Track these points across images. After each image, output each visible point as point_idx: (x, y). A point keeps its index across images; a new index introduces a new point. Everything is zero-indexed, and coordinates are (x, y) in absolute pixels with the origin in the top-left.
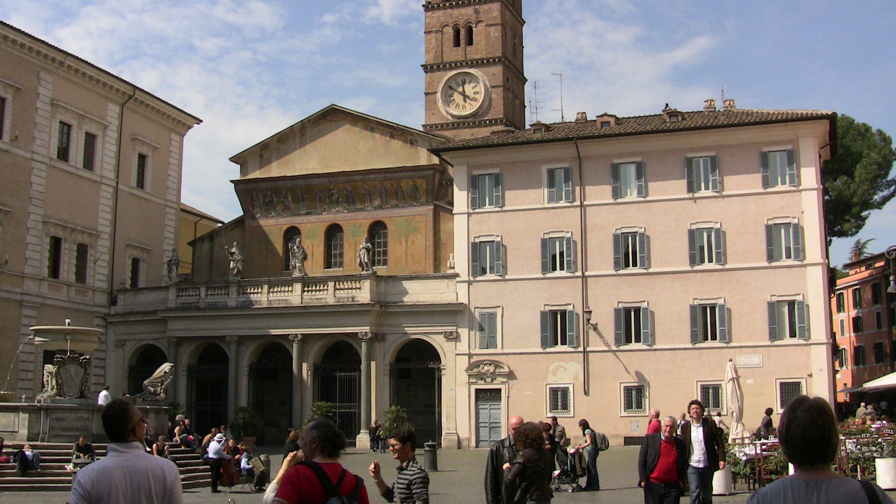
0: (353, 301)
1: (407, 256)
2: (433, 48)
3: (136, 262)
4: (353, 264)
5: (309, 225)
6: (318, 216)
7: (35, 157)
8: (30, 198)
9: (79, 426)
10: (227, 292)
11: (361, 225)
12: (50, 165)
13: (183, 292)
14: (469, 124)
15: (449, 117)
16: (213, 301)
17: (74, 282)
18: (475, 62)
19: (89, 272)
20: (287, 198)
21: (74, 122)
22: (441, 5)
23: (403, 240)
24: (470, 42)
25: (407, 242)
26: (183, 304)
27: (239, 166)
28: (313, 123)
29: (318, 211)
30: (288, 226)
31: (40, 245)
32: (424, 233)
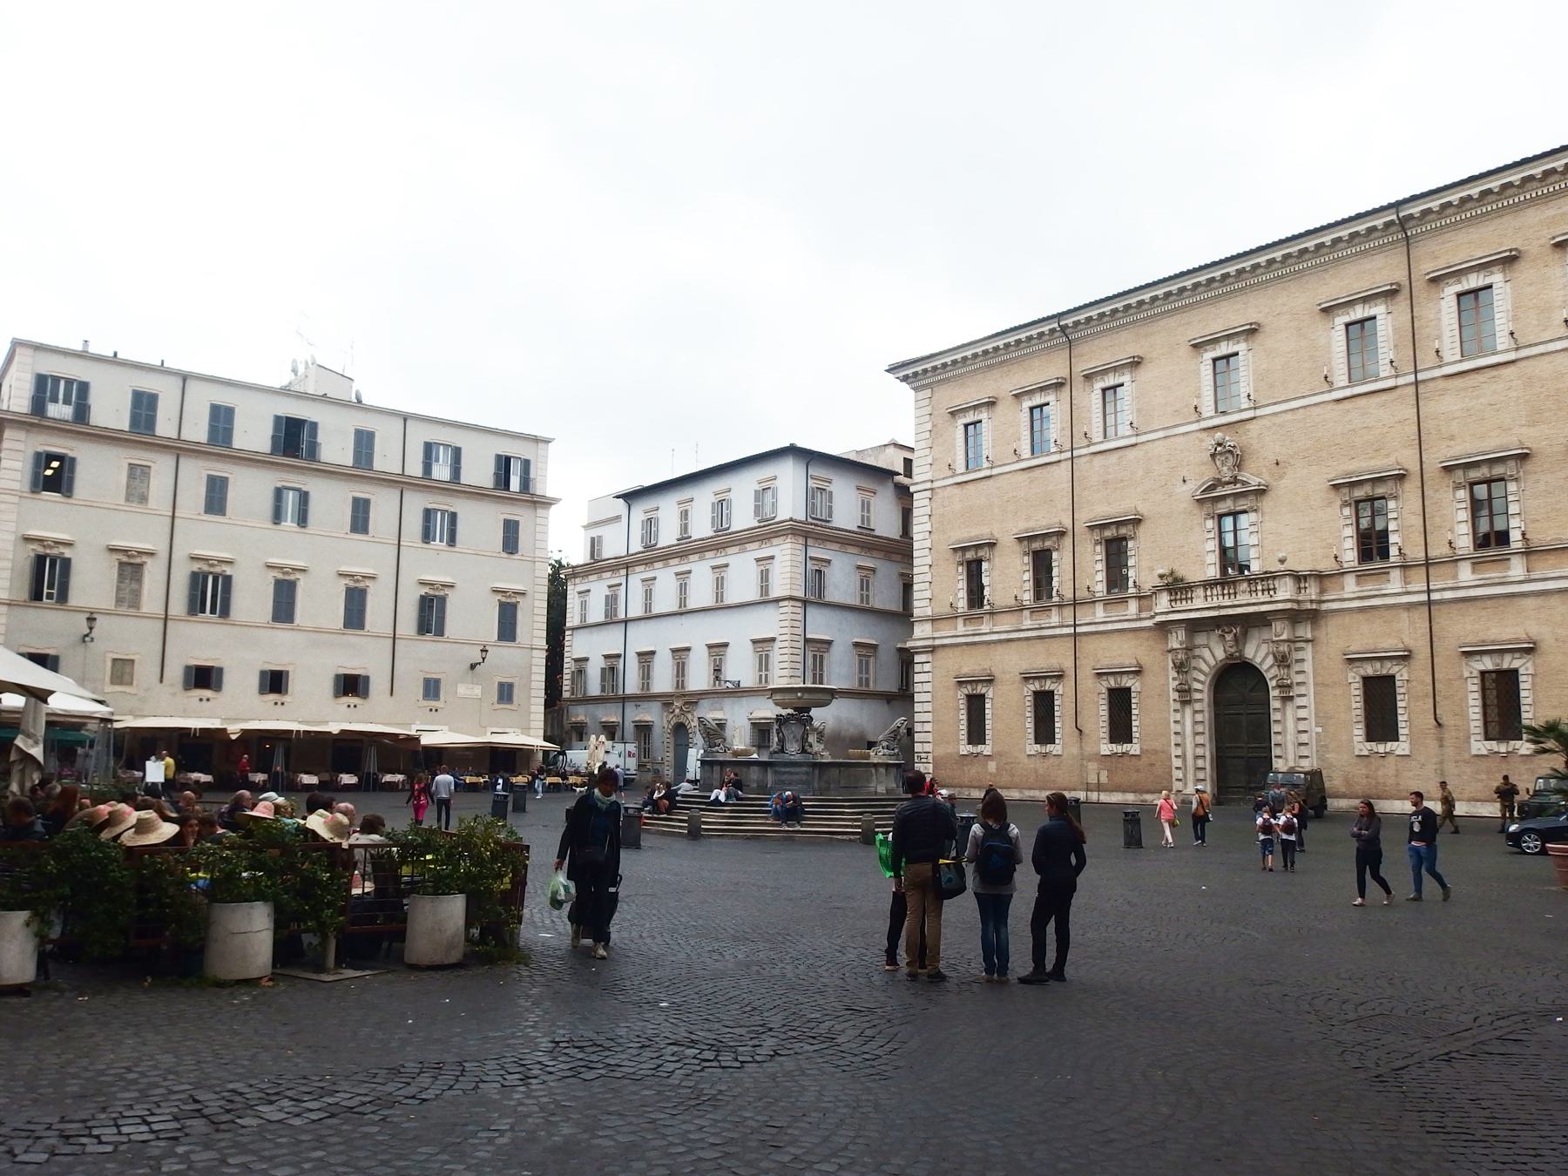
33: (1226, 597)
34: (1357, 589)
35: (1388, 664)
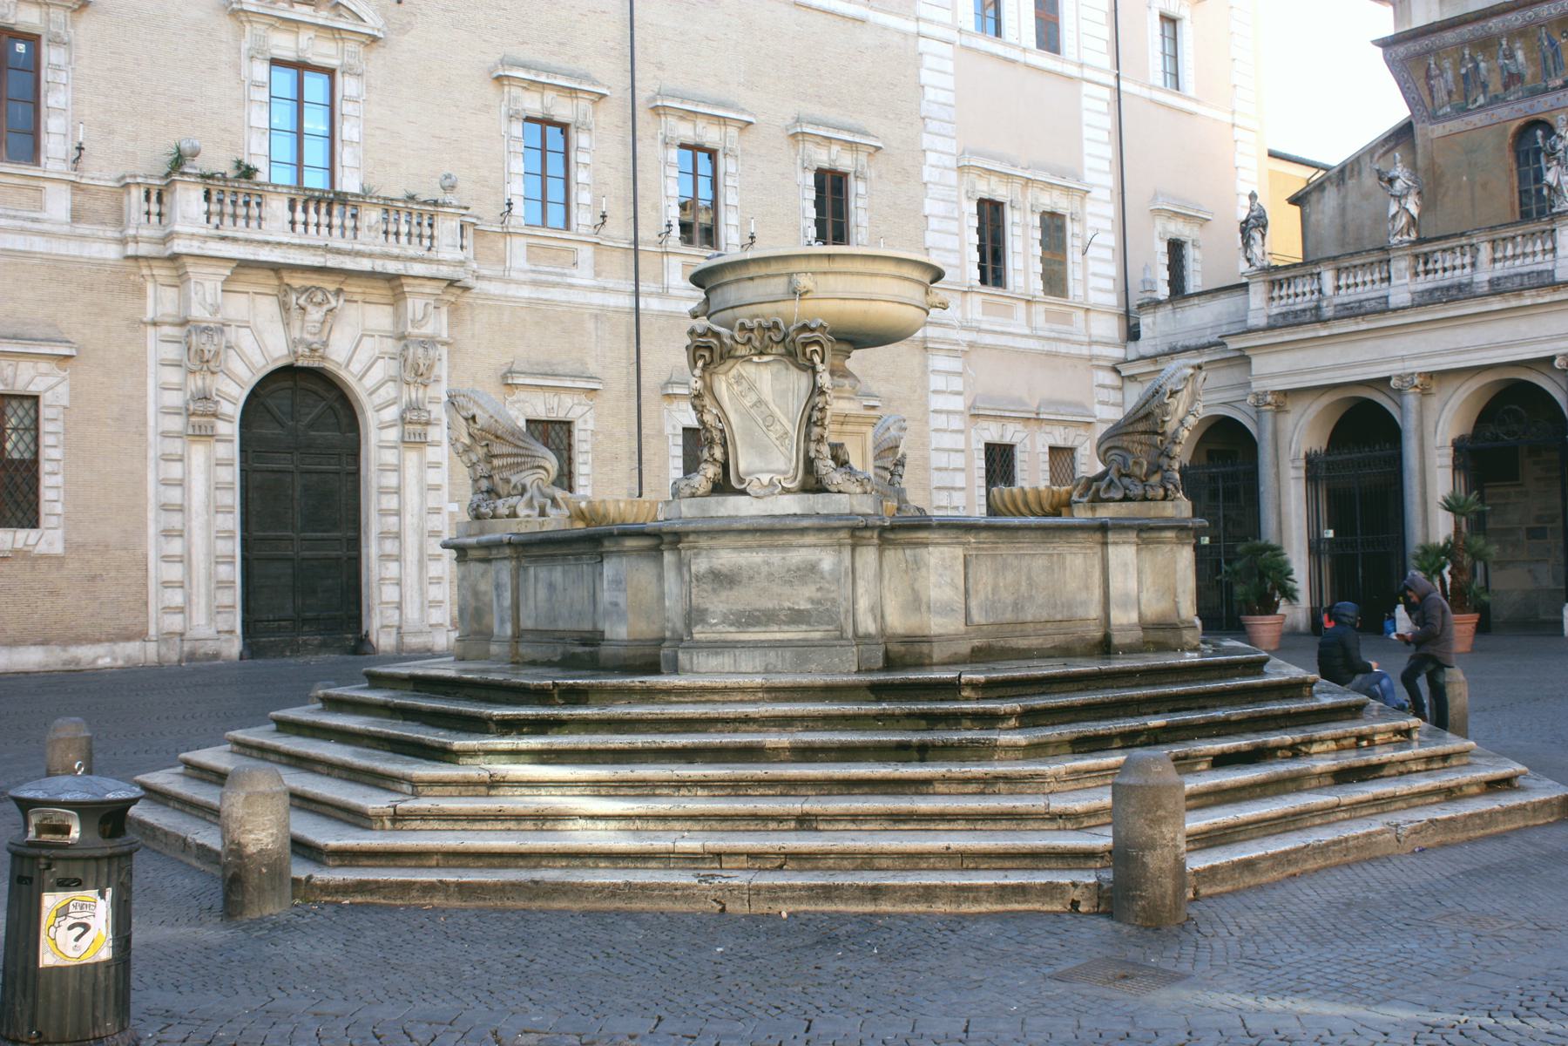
3: (1176, 248)
7: (924, 28)
8: (923, 119)
9: (804, 605)
10: (1385, 275)
12: (962, 46)
13: (1281, 286)
16: (1353, 298)
17: (1042, 294)
19: (1074, 273)
20: (1512, 56)
27: (1391, 8)
30: (1516, 124)
31: (957, 219)
33: (241, 222)
34: (527, 266)
35: (568, 400)
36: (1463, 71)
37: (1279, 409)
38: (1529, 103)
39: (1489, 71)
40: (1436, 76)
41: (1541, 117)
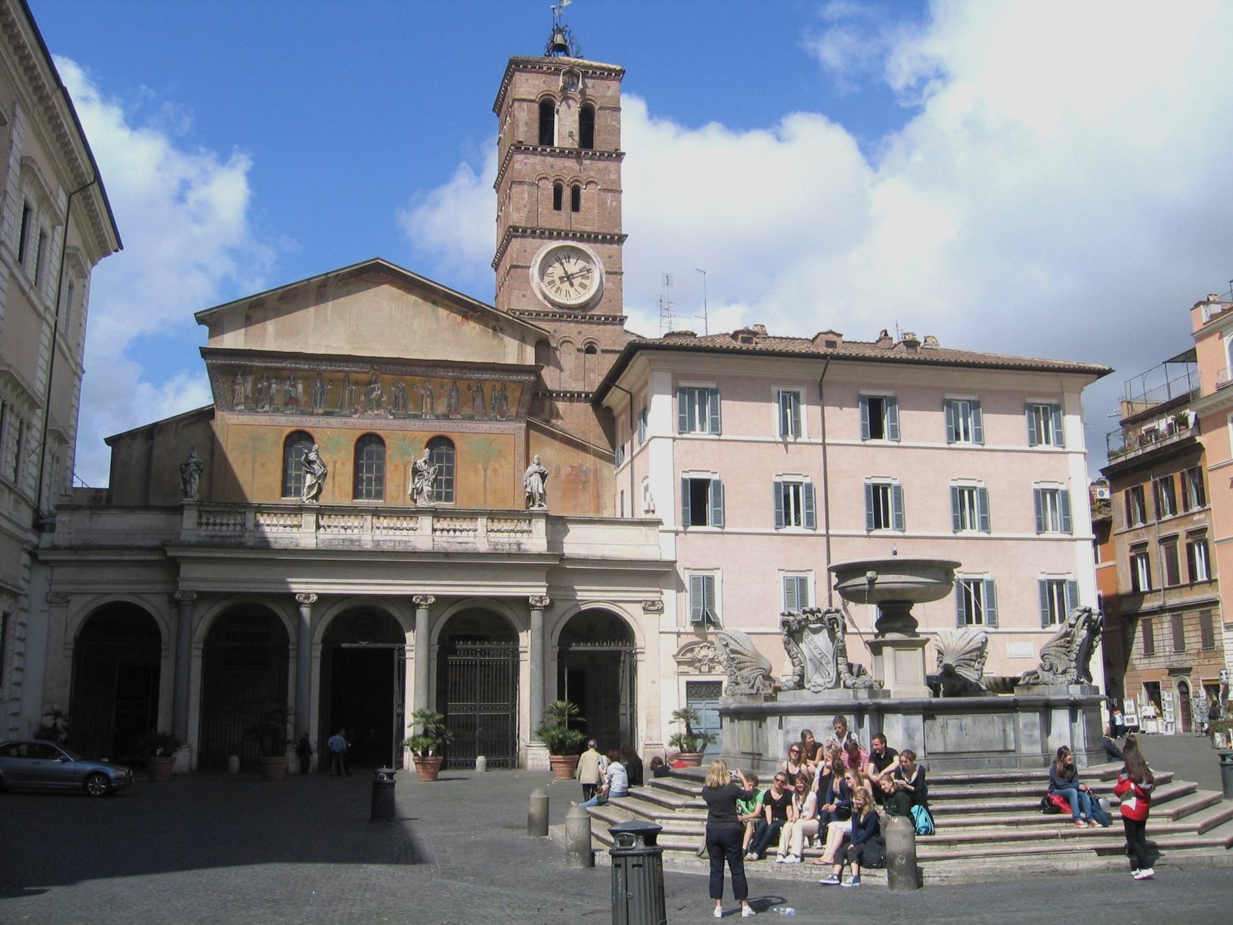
0: (519, 549)
1: (485, 490)
2: (525, 206)
4: (401, 495)
5: (328, 431)
6: (344, 420)
11: (415, 438)
14: (576, 317)
15: (546, 303)
18: (585, 235)
20: (295, 386)
21: (34, 205)
22: (539, 149)
23: (480, 466)
24: (576, 207)
25: (485, 471)
26: (213, 537)
28: (340, 281)
29: (348, 412)
30: (293, 429)
32: (511, 459)
36: (260, 386)
37: (194, 604)
38: (299, 418)
39: (277, 391)
40: (239, 384)
41: (307, 430)
